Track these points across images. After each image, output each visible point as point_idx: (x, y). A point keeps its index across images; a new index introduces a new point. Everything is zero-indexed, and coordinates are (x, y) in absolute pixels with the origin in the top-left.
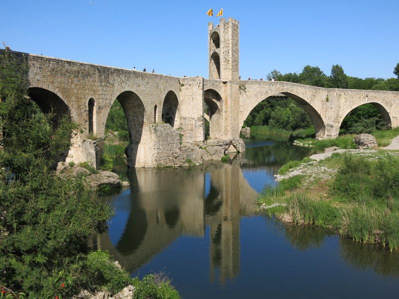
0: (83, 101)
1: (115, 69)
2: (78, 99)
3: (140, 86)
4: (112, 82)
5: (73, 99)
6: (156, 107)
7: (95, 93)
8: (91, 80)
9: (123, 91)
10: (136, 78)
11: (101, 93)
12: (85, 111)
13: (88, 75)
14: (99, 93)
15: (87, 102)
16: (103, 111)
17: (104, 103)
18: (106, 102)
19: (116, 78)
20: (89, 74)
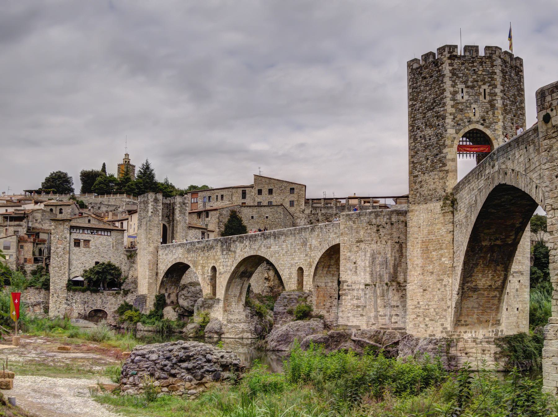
0: (206, 268)
1: (237, 237)
2: (203, 267)
3: (270, 248)
4: (232, 249)
5: (200, 267)
6: (301, 270)
7: (216, 261)
8: (214, 251)
9: (246, 255)
10: (265, 239)
11: (222, 260)
12: (208, 276)
13: (212, 247)
14: (219, 261)
15: (210, 269)
16: (223, 276)
17: (225, 270)
18: (227, 268)
19: (238, 245)
20: (212, 247)
